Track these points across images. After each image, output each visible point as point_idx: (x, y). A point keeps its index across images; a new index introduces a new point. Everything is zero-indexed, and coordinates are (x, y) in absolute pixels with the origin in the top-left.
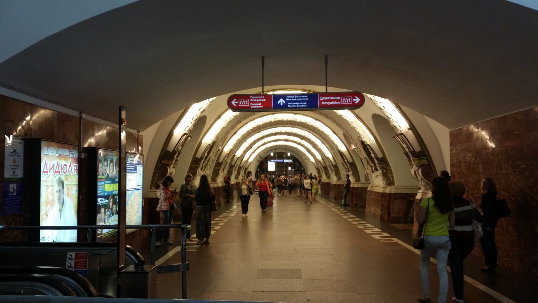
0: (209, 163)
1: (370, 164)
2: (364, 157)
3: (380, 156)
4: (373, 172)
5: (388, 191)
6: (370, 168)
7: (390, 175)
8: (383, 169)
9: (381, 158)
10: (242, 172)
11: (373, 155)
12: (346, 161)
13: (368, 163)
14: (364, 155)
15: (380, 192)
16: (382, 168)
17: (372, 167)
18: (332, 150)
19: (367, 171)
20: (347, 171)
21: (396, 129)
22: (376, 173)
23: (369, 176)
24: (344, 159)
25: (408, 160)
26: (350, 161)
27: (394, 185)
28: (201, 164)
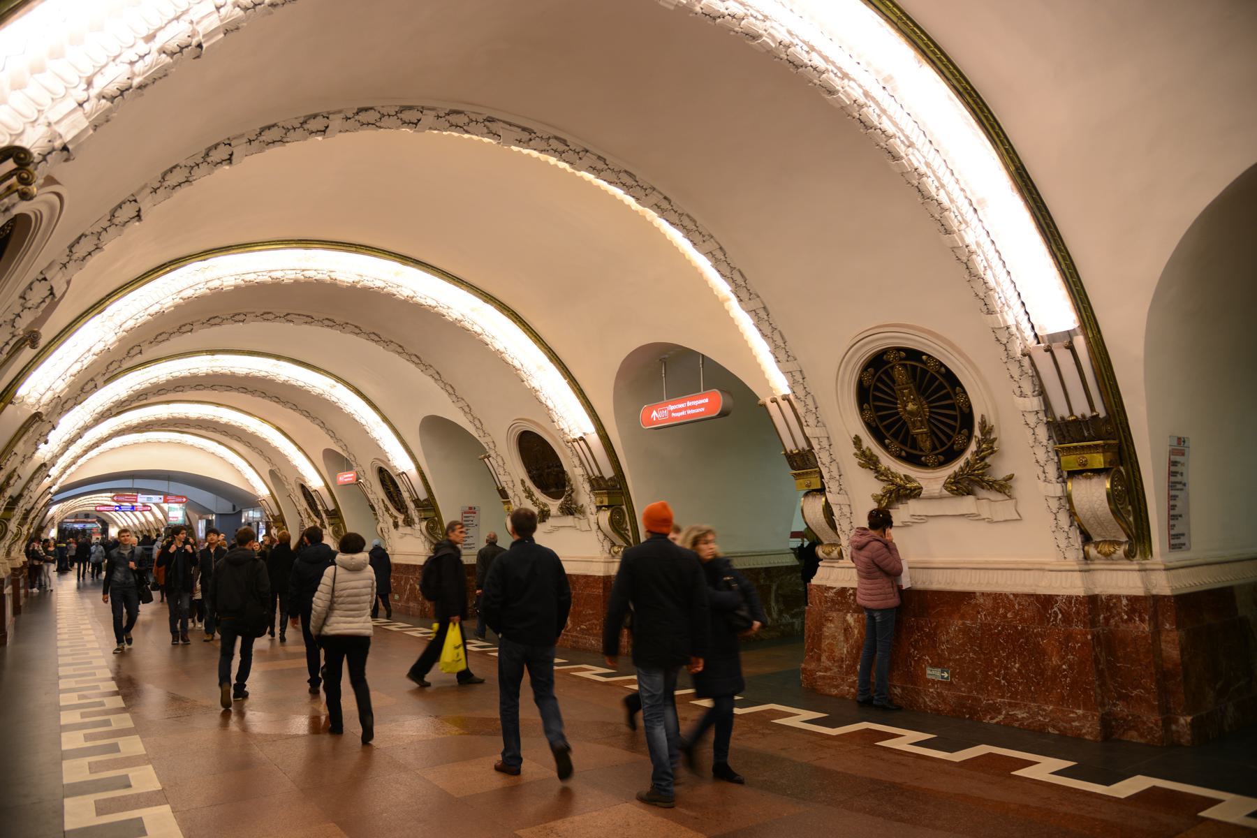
3: (423, 495)
4: (396, 525)
7: (440, 532)
14: (377, 493)
16: (426, 519)
17: (396, 517)
19: (381, 525)
21: (487, 448)
23: (386, 535)
25: (504, 502)
26: (331, 507)
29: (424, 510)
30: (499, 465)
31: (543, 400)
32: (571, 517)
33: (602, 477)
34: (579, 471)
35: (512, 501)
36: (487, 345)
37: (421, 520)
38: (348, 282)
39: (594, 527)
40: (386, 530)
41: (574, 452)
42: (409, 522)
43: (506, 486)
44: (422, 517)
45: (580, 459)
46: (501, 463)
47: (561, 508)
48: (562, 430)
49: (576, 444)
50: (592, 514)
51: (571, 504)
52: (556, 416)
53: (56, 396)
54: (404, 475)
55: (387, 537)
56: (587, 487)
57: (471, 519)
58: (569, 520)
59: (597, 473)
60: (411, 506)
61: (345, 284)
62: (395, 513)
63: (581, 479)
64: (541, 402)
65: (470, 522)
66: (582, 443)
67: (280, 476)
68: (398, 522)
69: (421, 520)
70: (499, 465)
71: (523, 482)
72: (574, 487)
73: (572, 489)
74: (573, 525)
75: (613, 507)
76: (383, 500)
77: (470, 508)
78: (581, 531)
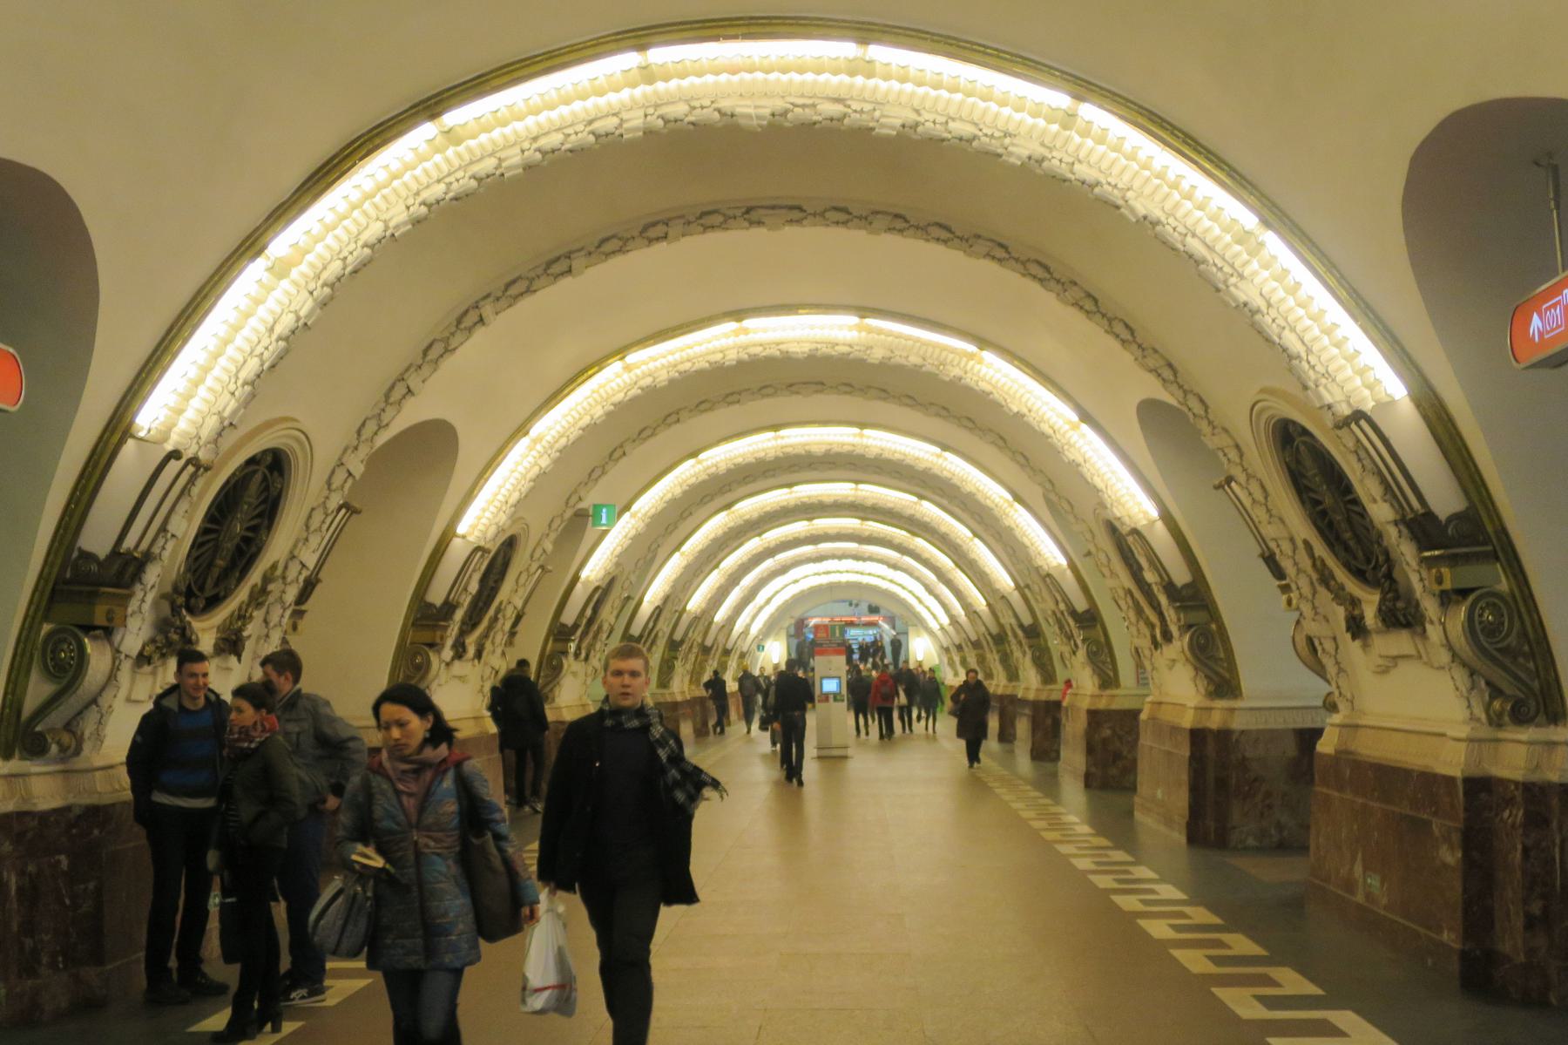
18: (1013, 564)
28: (449, 631)
30: (1254, 501)
31: (1273, 331)
35: (1293, 586)
36: (1118, 207)
38: (759, 117)
41: (1367, 462)
43: (1277, 551)
45: (1383, 481)
46: (1259, 495)
48: (1329, 407)
52: (1311, 373)
61: (755, 122)
64: (1268, 340)
70: (1254, 501)
74: (1413, 652)
75: (1471, 598)
78: (1432, 667)
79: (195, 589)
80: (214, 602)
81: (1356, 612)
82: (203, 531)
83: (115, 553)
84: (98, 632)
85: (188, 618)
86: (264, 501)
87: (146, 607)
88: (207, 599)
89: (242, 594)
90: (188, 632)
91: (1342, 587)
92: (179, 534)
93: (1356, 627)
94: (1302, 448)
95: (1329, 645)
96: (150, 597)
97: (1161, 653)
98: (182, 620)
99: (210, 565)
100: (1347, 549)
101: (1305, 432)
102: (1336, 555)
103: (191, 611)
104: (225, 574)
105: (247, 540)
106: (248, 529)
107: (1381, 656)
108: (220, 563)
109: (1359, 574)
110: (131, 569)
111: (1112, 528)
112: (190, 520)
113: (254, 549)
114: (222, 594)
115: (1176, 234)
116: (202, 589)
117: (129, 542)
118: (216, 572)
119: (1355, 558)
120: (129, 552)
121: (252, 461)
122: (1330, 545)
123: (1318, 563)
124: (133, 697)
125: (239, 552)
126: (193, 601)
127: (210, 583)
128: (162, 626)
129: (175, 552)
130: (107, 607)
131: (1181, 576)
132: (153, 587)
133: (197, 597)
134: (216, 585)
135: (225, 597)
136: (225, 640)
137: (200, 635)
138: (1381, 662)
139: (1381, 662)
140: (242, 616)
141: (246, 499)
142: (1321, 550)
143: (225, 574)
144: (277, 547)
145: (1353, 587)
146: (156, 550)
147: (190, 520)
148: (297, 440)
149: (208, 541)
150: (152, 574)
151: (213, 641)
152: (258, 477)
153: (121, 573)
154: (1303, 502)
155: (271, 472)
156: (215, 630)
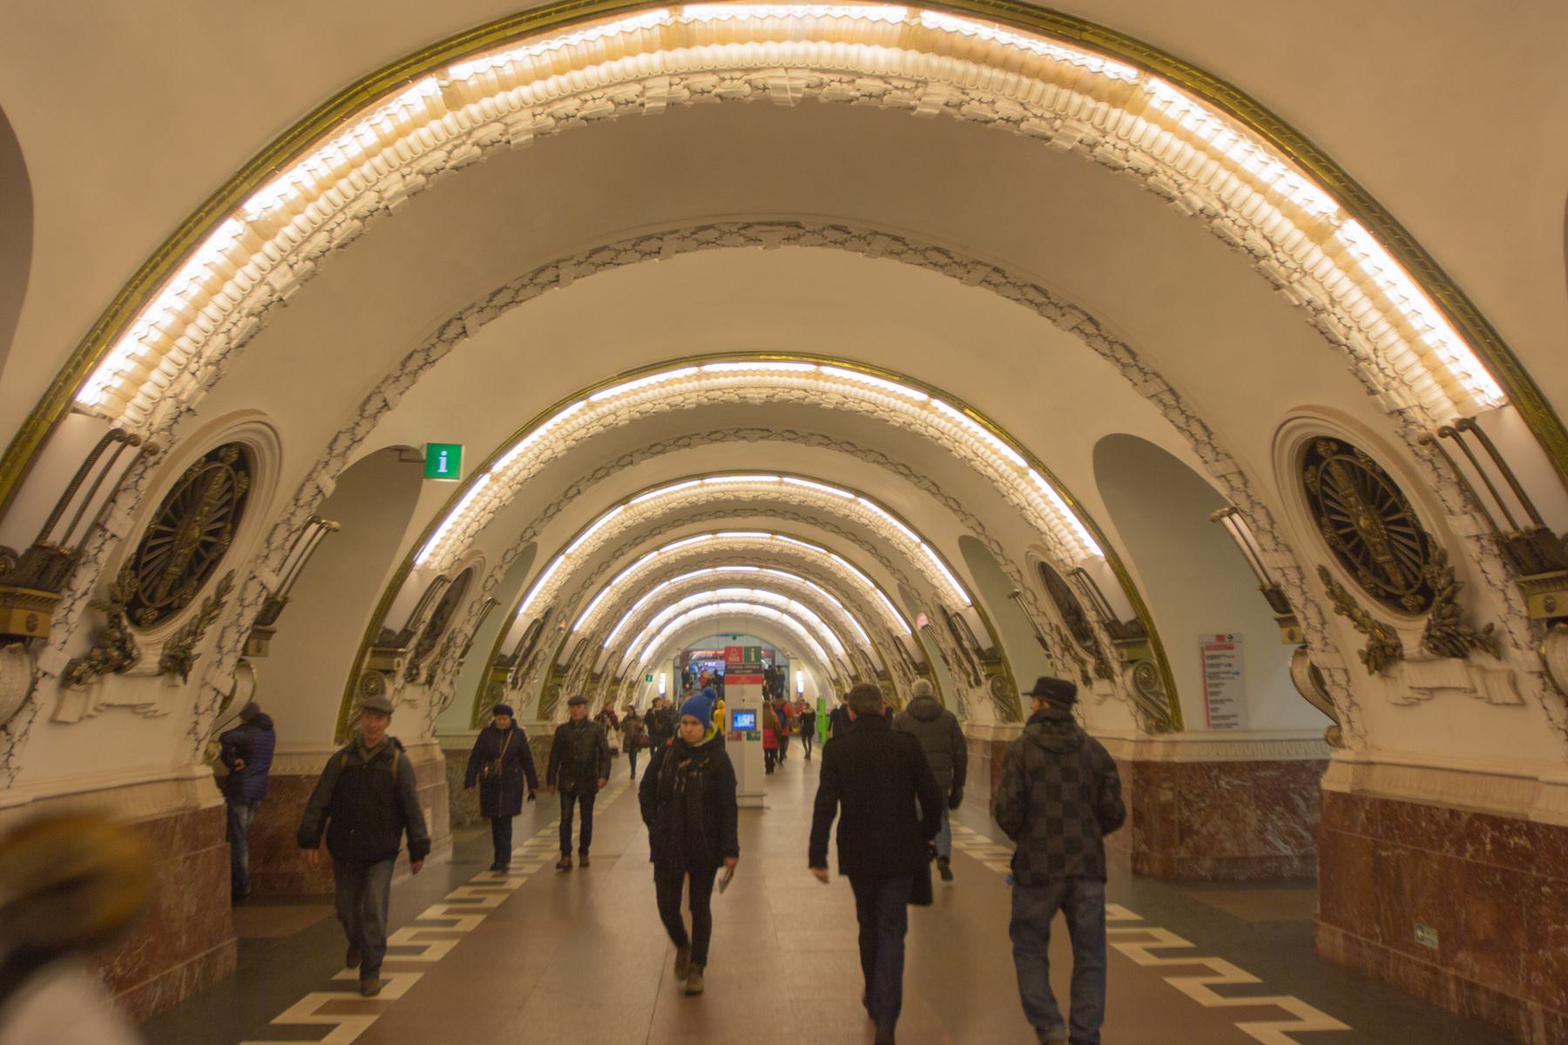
0: (450, 654)
1: (1073, 653)
2: (1050, 624)
4: (1087, 680)
5: (1157, 752)
6: (1076, 668)
7: (1164, 691)
8: (1136, 665)
9: (1131, 622)
10: (599, 691)
11: (1091, 617)
12: (966, 644)
13: (1067, 648)
15: (1153, 759)
20: (973, 683)
22: (1101, 686)
24: (961, 638)
27: (1179, 729)
29: (1127, 645)
32: (1456, 664)
33: (1543, 532)
34: (1463, 525)
37: (1125, 665)
39: (1531, 686)
40: (965, 692)
42: (1104, 671)
44: (1125, 659)
47: (1429, 637)
49: (1448, 443)
50: (1516, 645)
51: (1456, 624)
53: (183, 407)
54: (1081, 574)
55: (965, 702)
56: (1495, 569)
57: (1224, 660)
58: (1452, 671)
59: (1524, 521)
60: (1104, 638)
62: (1083, 654)
63: (1472, 548)
64: (1332, 341)
65: (1223, 669)
66: (1467, 436)
67: (908, 589)
68: (1087, 672)
69: (1125, 665)
71: (1324, 573)
72: (1458, 578)
73: (1452, 581)
76: (1057, 627)
77: (1220, 638)
78: (1490, 702)
79: (144, 600)
80: (167, 612)
81: (1391, 641)
82: (152, 534)
83: (37, 547)
84: (17, 645)
85: (129, 630)
86: (227, 504)
87: (74, 617)
88: (160, 610)
89: (194, 609)
90: (129, 645)
91: (1366, 615)
92: (122, 534)
93: (1383, 656)
94: (1336, 469)
95: (1340, 677)
96: (80, 606)
97: (1091, 688)
98: (122, 630)
99: (163, 572)
100: (1378, 571)
101: (1345, 448)
102: (1359, 580)
103: (136, 622)
104: (180, 582)
105: (207, 546)
106: (209, 533)
107: (1411, 688)
108: (174, 570)
109: (1391, 600)
110: (57, 567)
111: (1046, 572)
112: (136, 518)
113: (214, 555)
114: (176, 604)
115: (1236, 227)
116: (151, 599)
117: (55, 537)
118: (169, 580)
119: (1388, 582)
120: (51, 548)
121: (212, 456)
122: (1352, 569)
123: (1337, 590)
124: (60, 718)
125: (198, 558)
126: (139, 612)
127: (161, 591)
128: (98, 638)
129: (116, 553)
130: (29, 612)
131: (1125, 613)
132: (85, 593)
133: (146, 607)
134: (170, 594)
135: (180, 608)
136: (173, 657)
137: (143, 650)
138: (1409, 693)
139: (1409, 693)
140: (195, 632)
141: (206, 500)
142: (1340, 575)
143: (180, 582)
144: (240, 554)
145: (1380, 613)
146: (91, 549)
147: (136, 518)
148: (261, 432)
149: (162, 545)
150: (84, 580)
151: (158, 659)
152: (221, 476)
153: (43, 571)
154: (1321, 526)
155: (237, 472)
156: (161, 645)
